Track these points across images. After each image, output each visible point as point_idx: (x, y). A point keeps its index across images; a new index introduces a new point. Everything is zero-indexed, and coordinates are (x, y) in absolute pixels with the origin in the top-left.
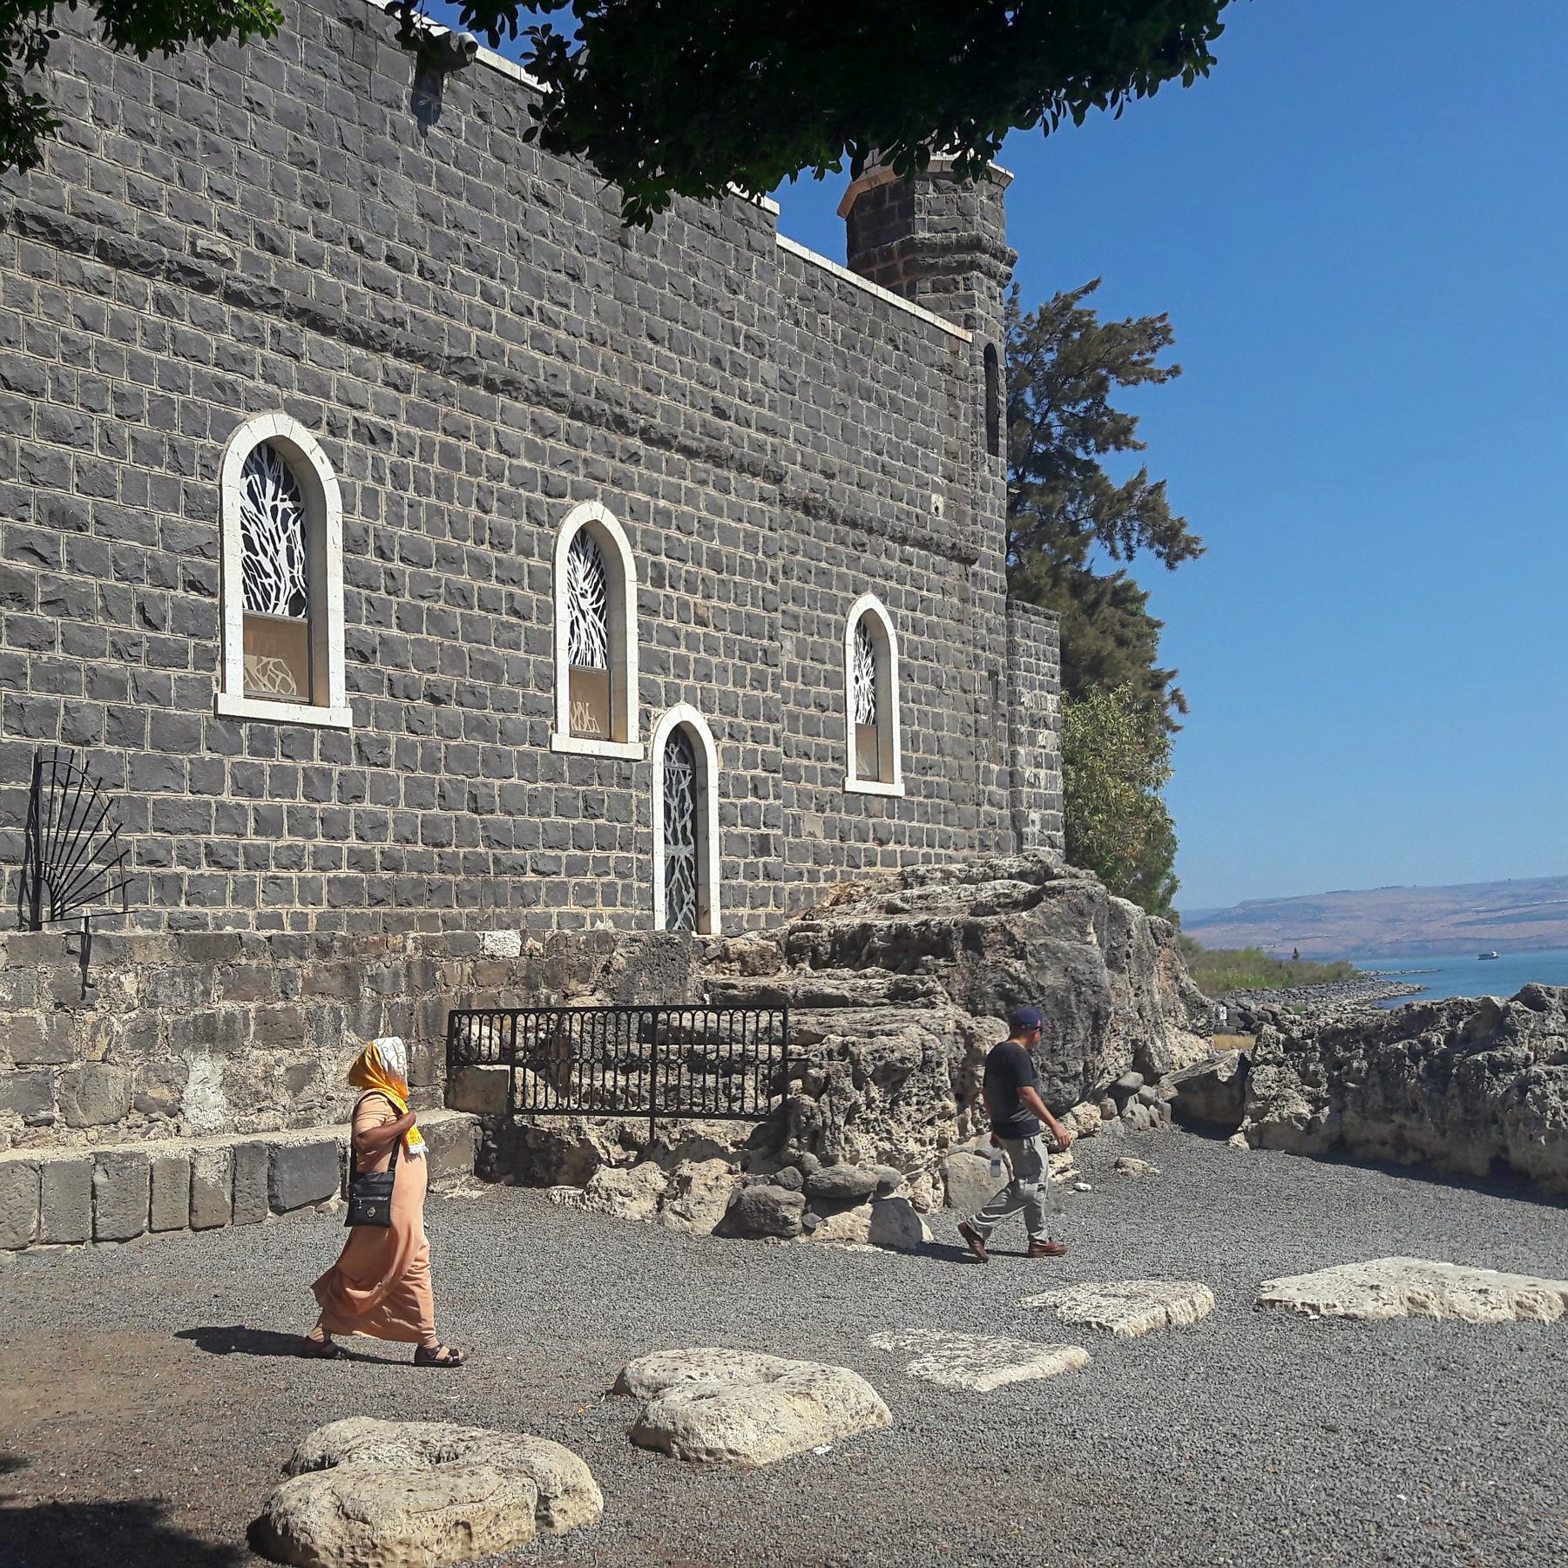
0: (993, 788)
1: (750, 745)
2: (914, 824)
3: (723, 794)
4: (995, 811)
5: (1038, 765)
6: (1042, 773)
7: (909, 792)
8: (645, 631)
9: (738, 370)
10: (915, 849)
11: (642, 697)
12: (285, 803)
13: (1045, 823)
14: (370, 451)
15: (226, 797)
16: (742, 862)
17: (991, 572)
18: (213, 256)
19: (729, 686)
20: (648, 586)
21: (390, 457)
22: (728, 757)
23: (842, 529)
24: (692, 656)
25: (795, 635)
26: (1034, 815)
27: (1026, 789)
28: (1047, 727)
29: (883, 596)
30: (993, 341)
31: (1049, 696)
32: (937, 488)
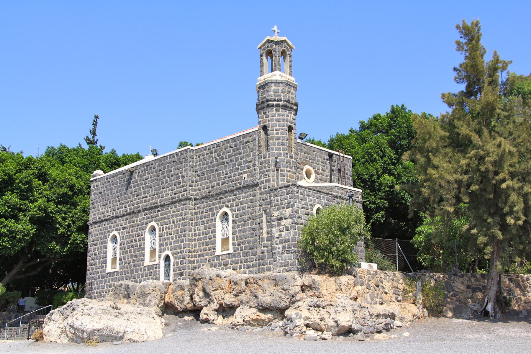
0: (265, 242)
1: (180, 254)
2: (237, 258)
3: (174, 266)
4: (266, 248)
5: (281, 231)
6: (283, 233)
7: (235, 251)
8: (160, 240)
9: (179, 183)
10: (237, 265)
11: (159, 252)
12: (112, 283)
13: (284, 247)
14: (123, 231)
15: (107, 283)
16: (177, 278)
17: (265, 184)
18: (108, 216)
19: (176, 244)
20: (161, 232)
21: (125, 230)
22: (176, 258)
23: (216, 197)
24: (168, 241)
25: (204, 225)
26: (278, 246)
27: (276, 240)
28: (285, 219)
29: (228, 207)
30: (265, 124)
31: (287, 210)
32: (245, 173)
